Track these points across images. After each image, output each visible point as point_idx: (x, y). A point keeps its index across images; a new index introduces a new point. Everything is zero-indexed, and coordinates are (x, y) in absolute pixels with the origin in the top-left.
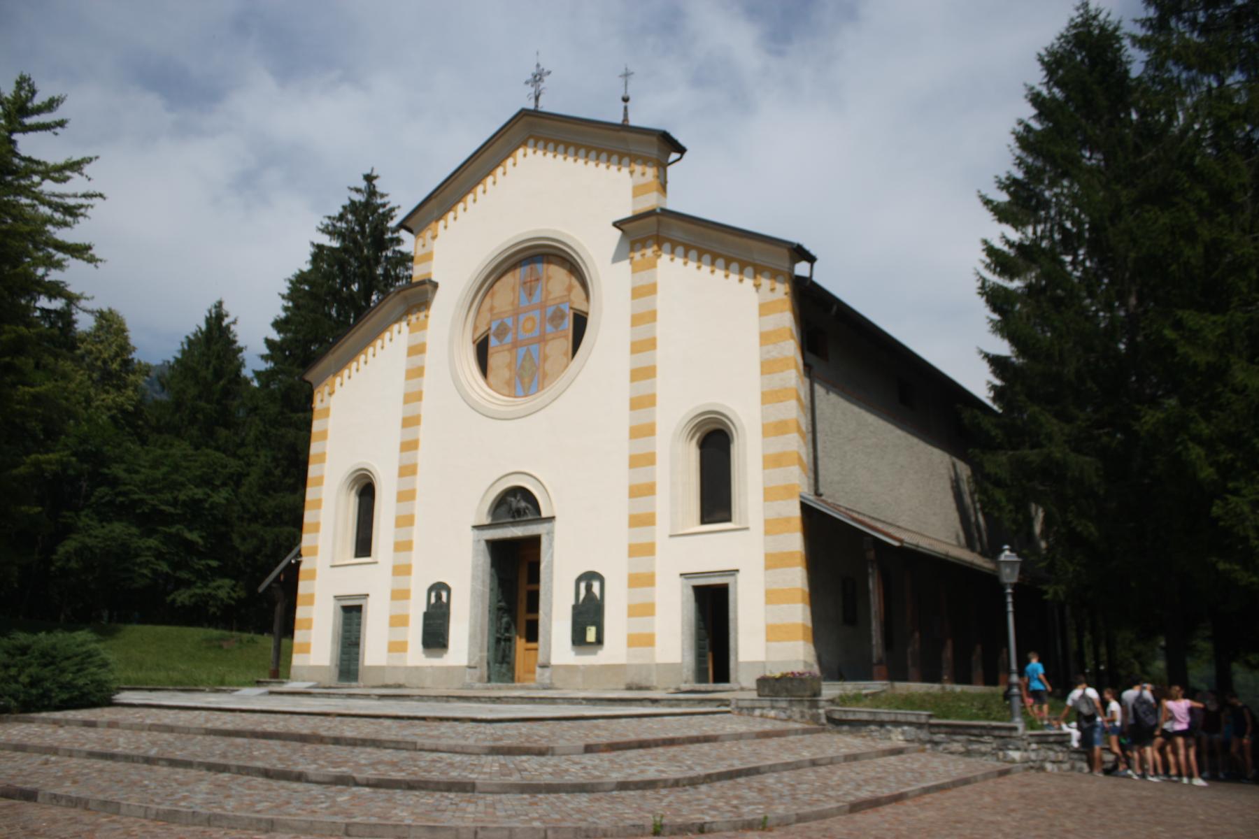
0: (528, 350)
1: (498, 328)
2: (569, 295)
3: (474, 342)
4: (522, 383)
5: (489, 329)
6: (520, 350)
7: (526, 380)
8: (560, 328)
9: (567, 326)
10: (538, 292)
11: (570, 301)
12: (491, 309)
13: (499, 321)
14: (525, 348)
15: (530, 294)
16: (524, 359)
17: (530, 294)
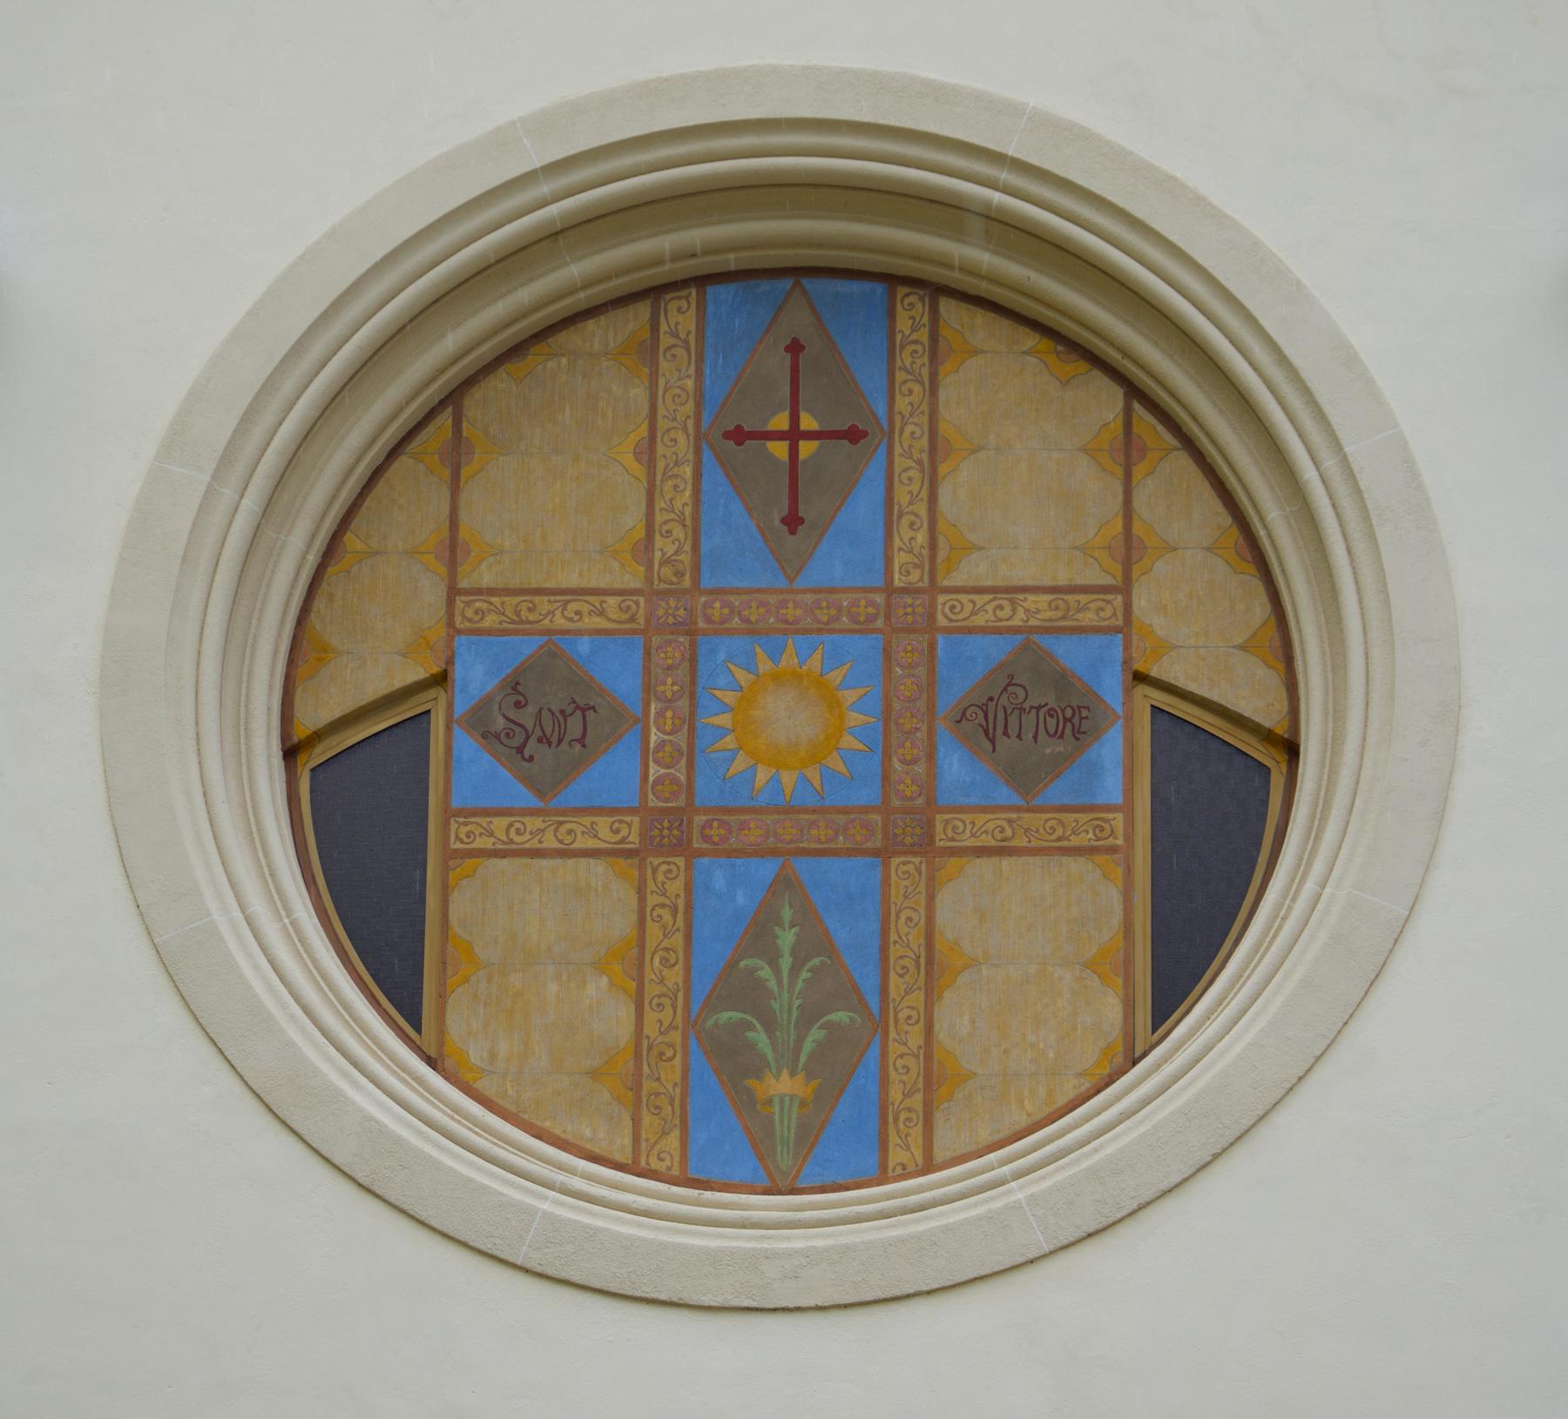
0: (784, 883)
1: (514, 686)
2: (1125, 588)
3: (291, 753)
4: (746, 1103)
5: (441, 679)
6: (717, 874)
7: (783, 1086)
8: (1057, 792)
9: (1111, 788)
10: (863, 506)
11: (1126, 626)
12: (453, 550)
13: (528, 646)
14: (767, 869)
15: (793, 521)
16: (758, 936)
17: (793, 521)
